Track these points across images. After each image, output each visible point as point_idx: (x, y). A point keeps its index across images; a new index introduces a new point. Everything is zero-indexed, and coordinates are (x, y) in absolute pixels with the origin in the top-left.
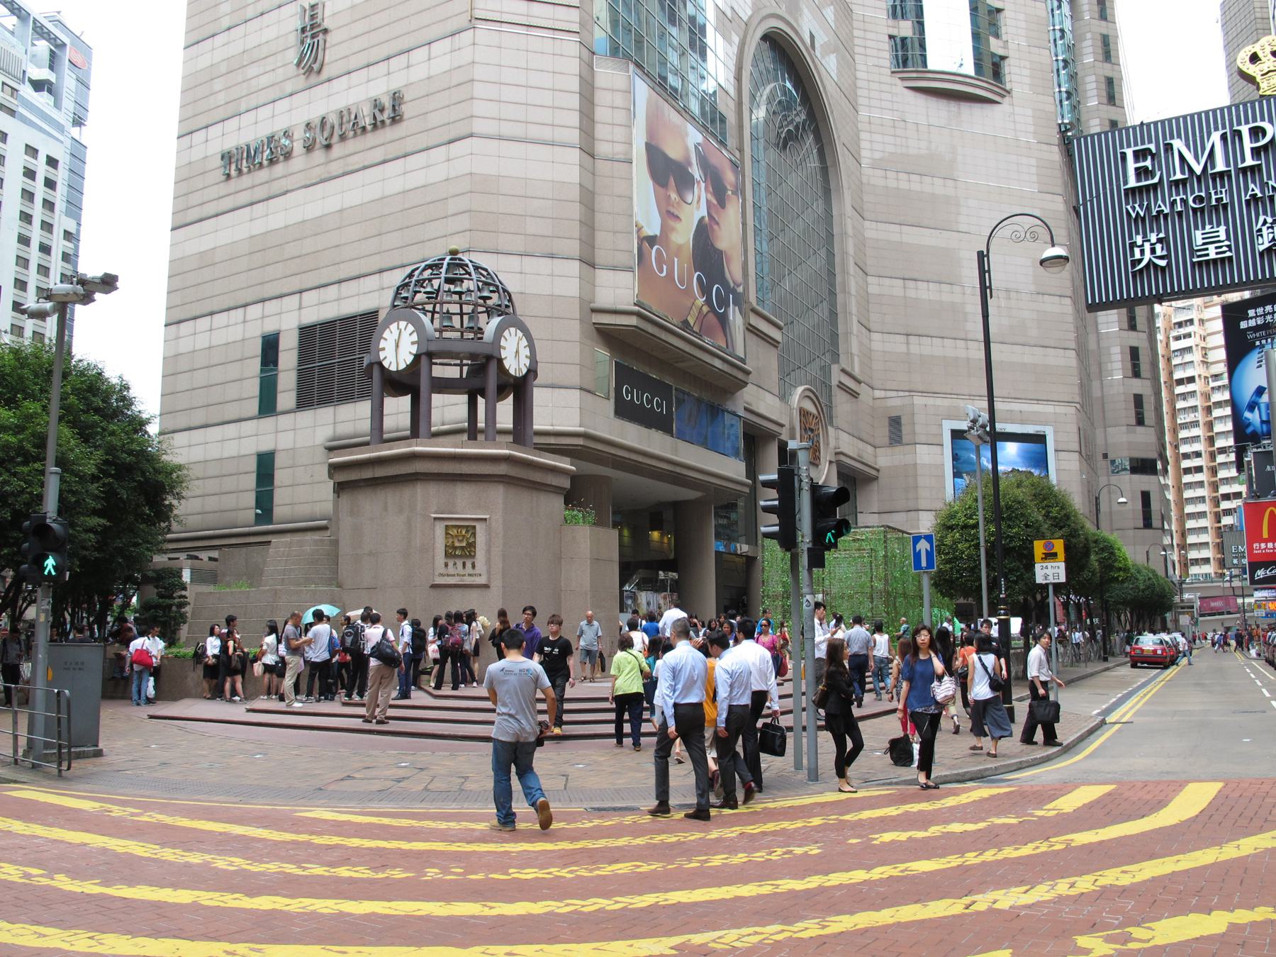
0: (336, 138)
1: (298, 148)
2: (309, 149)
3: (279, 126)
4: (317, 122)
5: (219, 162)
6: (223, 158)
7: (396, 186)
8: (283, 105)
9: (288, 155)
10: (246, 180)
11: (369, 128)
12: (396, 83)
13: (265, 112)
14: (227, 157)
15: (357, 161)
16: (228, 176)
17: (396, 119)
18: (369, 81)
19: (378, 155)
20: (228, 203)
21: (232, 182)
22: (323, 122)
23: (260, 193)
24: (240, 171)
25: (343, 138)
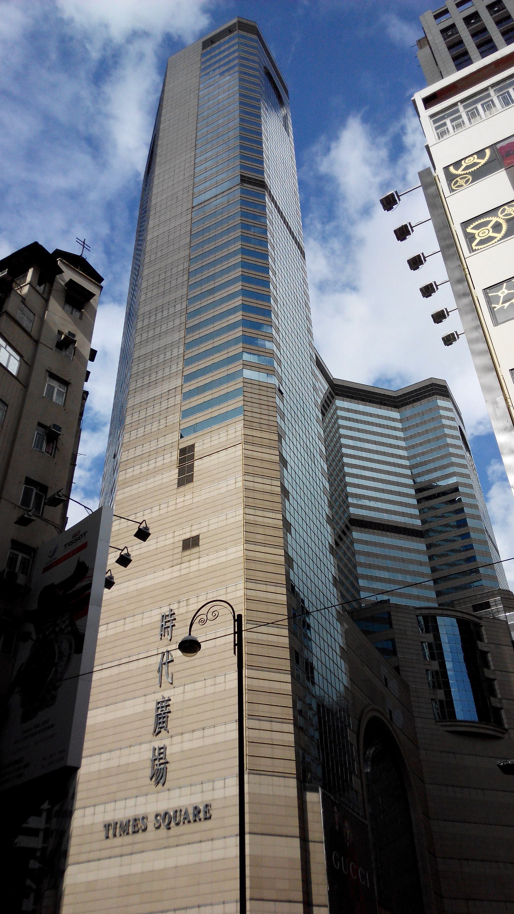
0: (173, 824)
1: (151, 826)
2: (158, 828)
3: (140, 811)
4: (162, 813)
5: (101, 828)
6: (105, 826)
7: (207, 857)
8: (141, 800)
9: (145, 830)
10: (118, 841)
11: (192, 821)
12: (207, 798)
13: (131, 802)
14: (107, 826)
15: (185, 839)
16: (107, 837)
17: (208, 818)
18: (191, 794)
19: (197, 837)
20: (106, 853)
21: (108, 841)
22: (166, 814)
23: (127, 850)
24: (115, 835)
25: (178, 824)
